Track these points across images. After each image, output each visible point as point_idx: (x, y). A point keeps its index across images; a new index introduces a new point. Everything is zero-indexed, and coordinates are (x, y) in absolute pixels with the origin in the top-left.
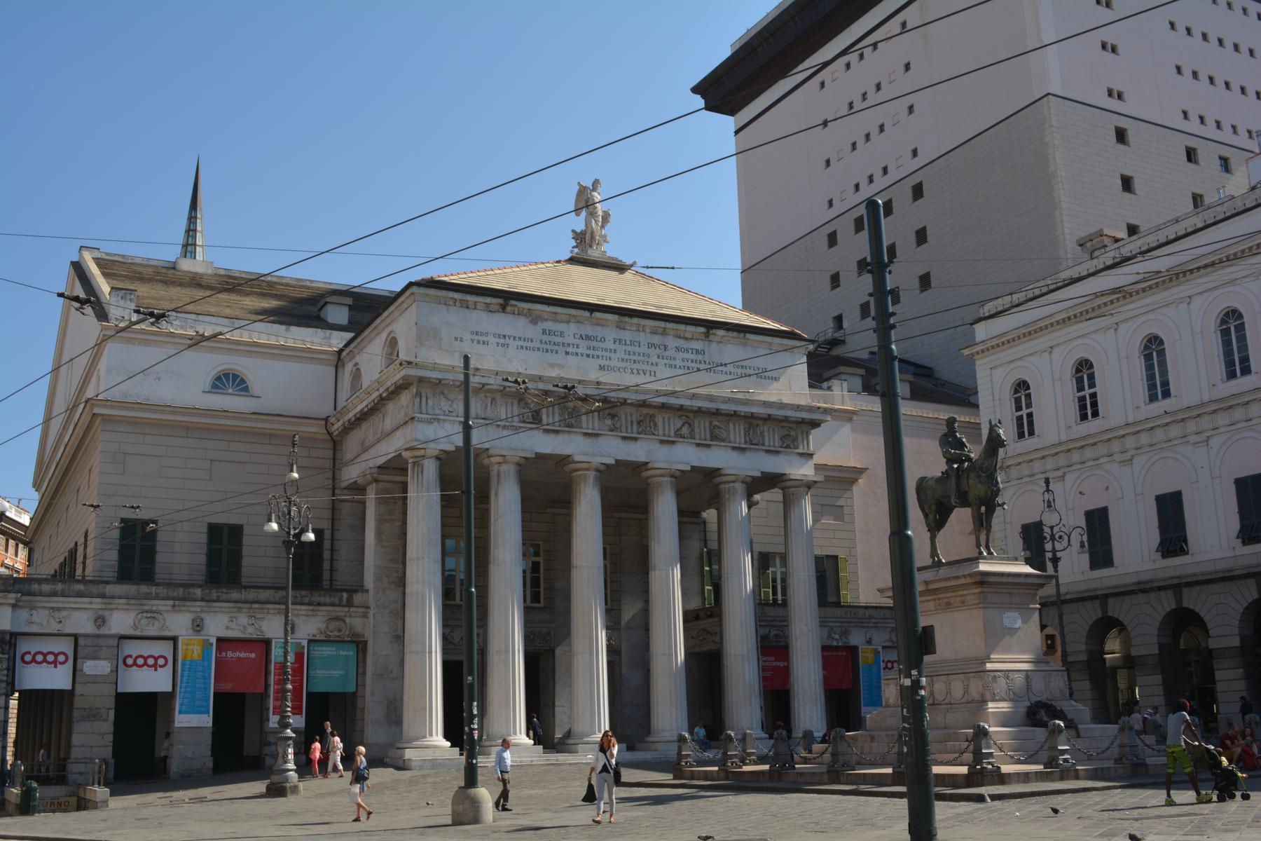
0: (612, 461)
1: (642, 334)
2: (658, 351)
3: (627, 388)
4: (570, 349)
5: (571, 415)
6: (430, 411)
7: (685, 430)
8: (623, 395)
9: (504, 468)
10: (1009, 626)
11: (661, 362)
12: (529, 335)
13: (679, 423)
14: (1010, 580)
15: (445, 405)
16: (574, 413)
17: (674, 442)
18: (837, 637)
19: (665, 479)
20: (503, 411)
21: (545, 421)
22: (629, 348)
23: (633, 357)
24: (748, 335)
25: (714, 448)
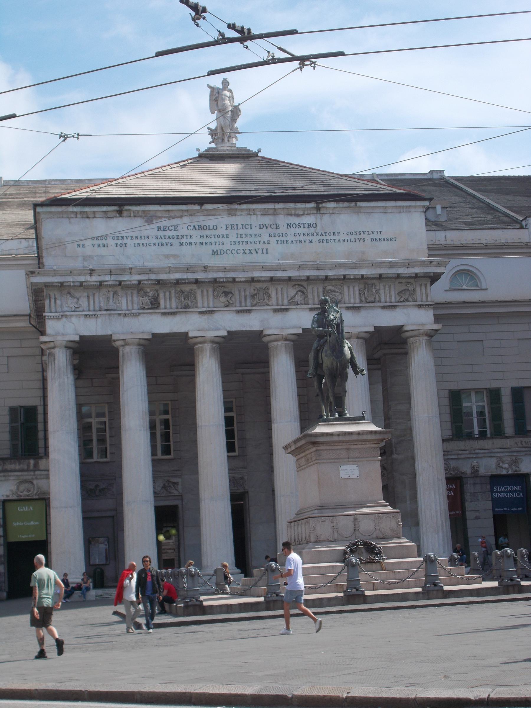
0: (225, 334)
1: (254, 217)
2: (270, 230)
3: (234, 269)
4: (184, 241)
5: (186, 297)
6: (59, 309)
7: (299, 298)
8: (231, 275)
9: (127, 349)
10: (347, 477)
11: (273, 239)
12: (145, 233)
13: (292, 292)
14: (341, 438)
15: (71, 303)
16: (191, 295)
17: (287, 310)
18: (506, 466)
19: (280, 343)
20: (124, 302)
21: (162, 305)
22: (241, 232)
23: (244, 239)
24: (359, 204)
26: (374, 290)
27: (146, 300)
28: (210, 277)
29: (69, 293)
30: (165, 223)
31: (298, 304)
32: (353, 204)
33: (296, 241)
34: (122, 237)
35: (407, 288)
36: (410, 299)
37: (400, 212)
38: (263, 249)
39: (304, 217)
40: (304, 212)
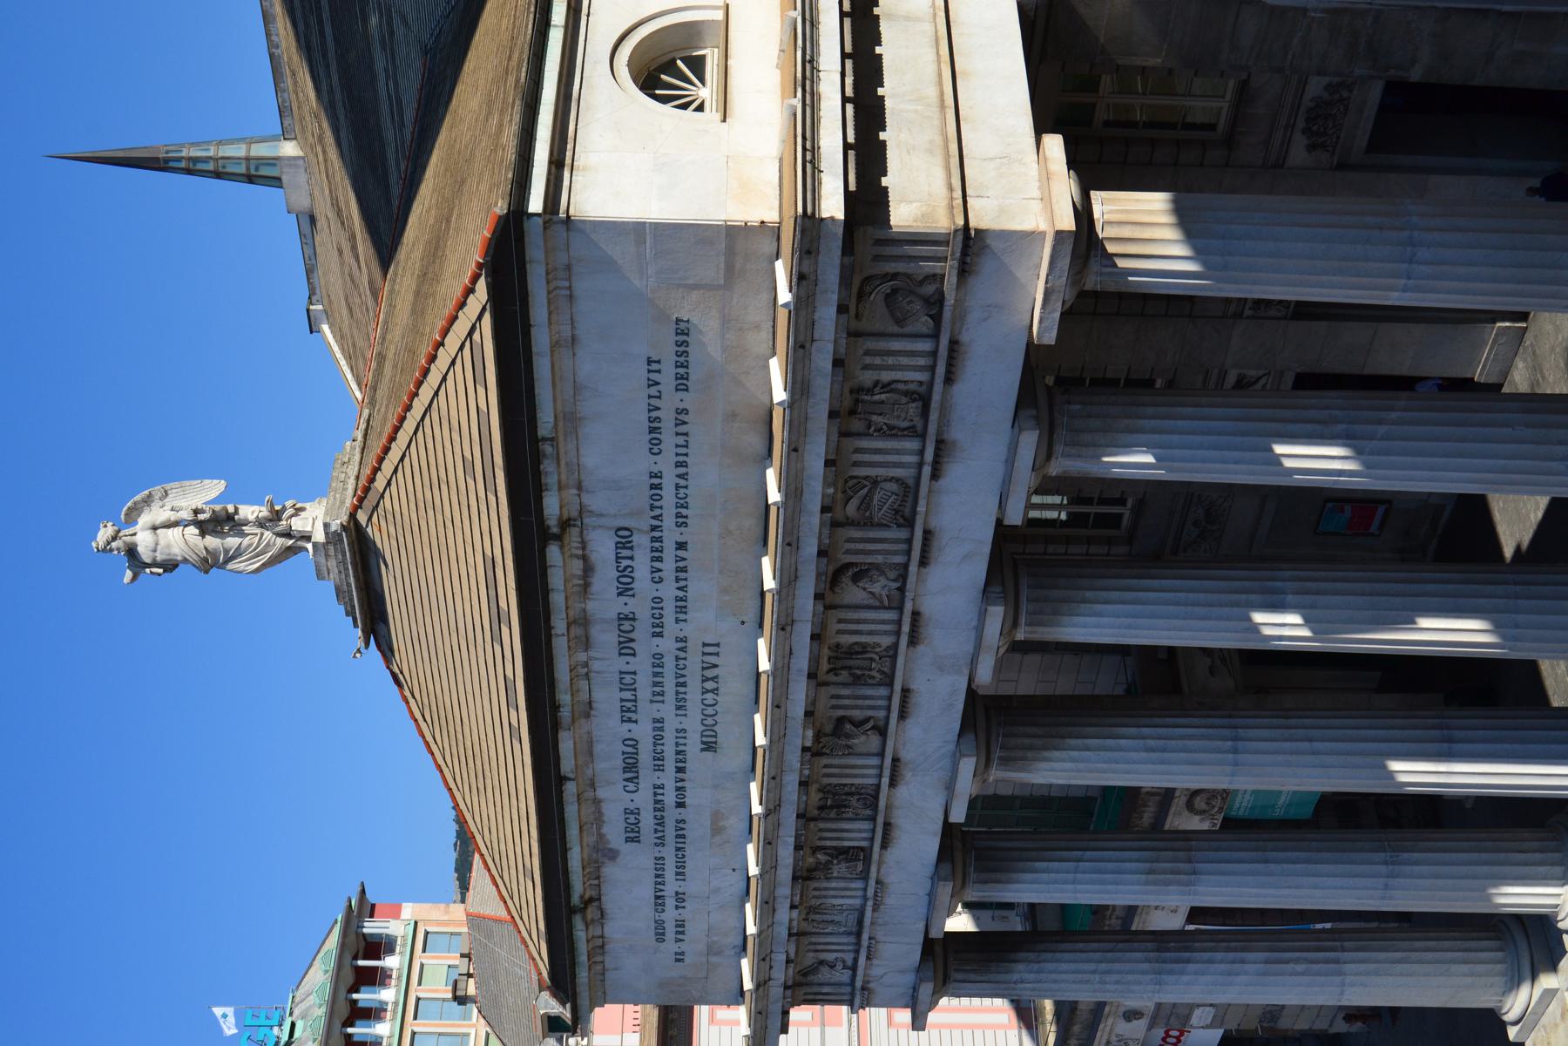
1: (595, 666)
2: (642, 632)
4: (670, 798)
7: (881, 586)
22: (644, 693)
25: (934, 523)
26: (877, 397)
27: (839, 868)
28: (795, 797)
29: (805, 975)
30: (614, 832)
31: (902, 590)
32: (547, 448)
33: (677, 580)
34: (657, 897)
35: (881, 298)
36: (929, 289)
37: (571, 296)
38: (704, 654)
39: (594, 557)
40: (577, 557)
